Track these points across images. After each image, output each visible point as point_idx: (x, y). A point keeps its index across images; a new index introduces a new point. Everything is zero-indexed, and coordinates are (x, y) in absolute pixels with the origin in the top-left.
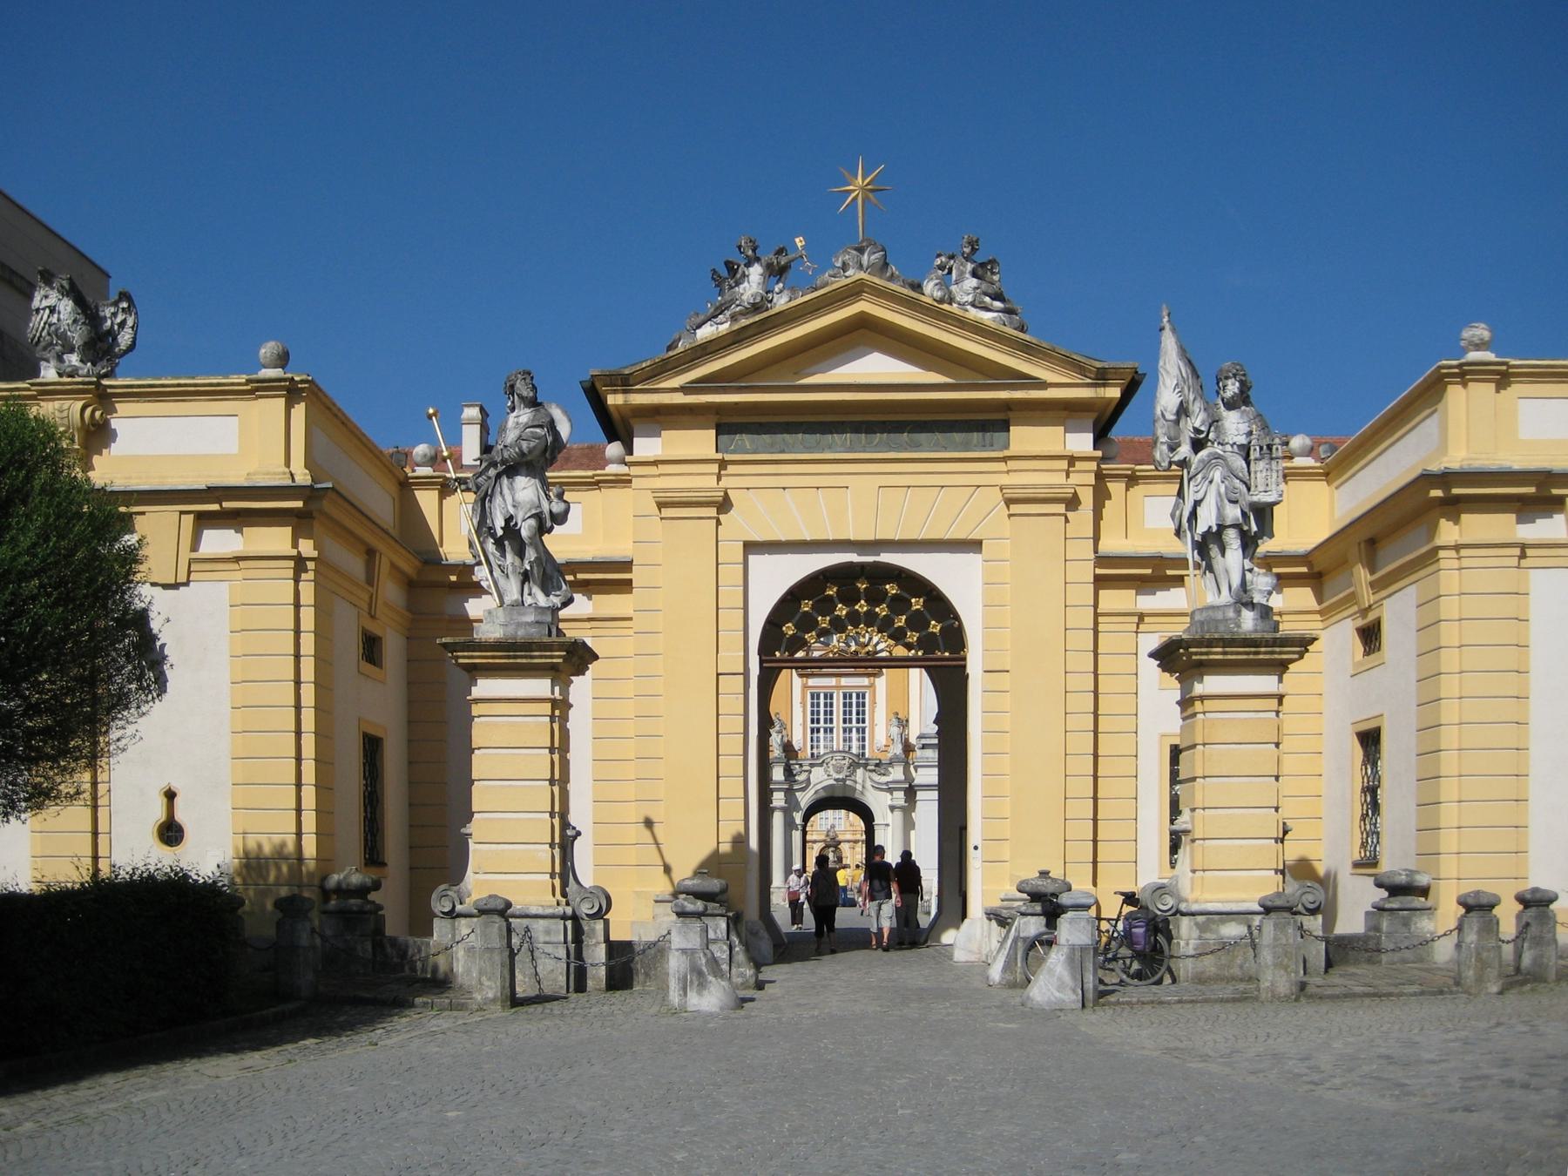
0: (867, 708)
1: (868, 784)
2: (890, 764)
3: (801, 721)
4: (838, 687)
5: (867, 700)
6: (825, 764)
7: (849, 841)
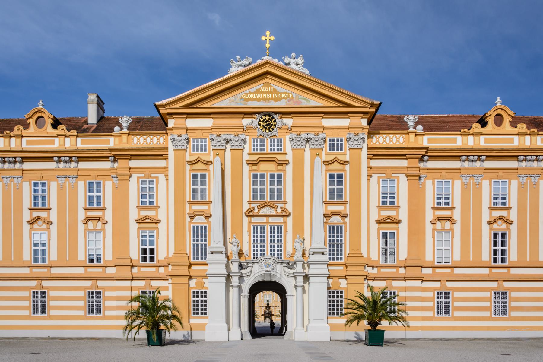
0: (283, 234)
1: (283, 274)
2: (295, 263)
3: (248, 241)
4: (267, 223)
5: (283, 230)
6: (260, 262)
7: (274, 306)
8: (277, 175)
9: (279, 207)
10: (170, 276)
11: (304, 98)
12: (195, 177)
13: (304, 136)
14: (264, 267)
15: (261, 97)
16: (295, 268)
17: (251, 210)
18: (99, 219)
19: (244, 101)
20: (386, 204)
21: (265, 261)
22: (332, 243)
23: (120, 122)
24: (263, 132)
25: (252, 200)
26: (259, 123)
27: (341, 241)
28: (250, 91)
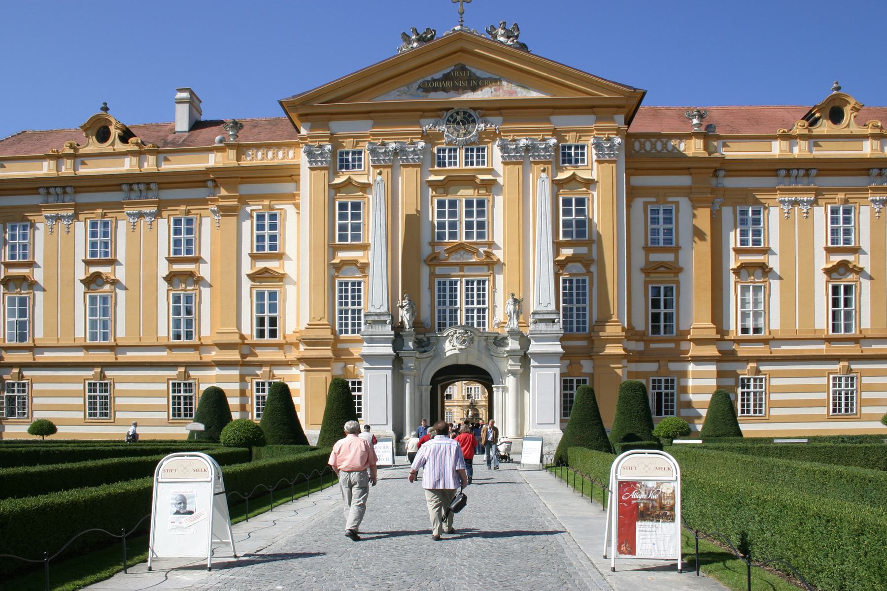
8: (477, 201)
10: (302, 360)
14: (455, 344)
19: (424, 91)
20: (659, 244)
27: (584, 301)
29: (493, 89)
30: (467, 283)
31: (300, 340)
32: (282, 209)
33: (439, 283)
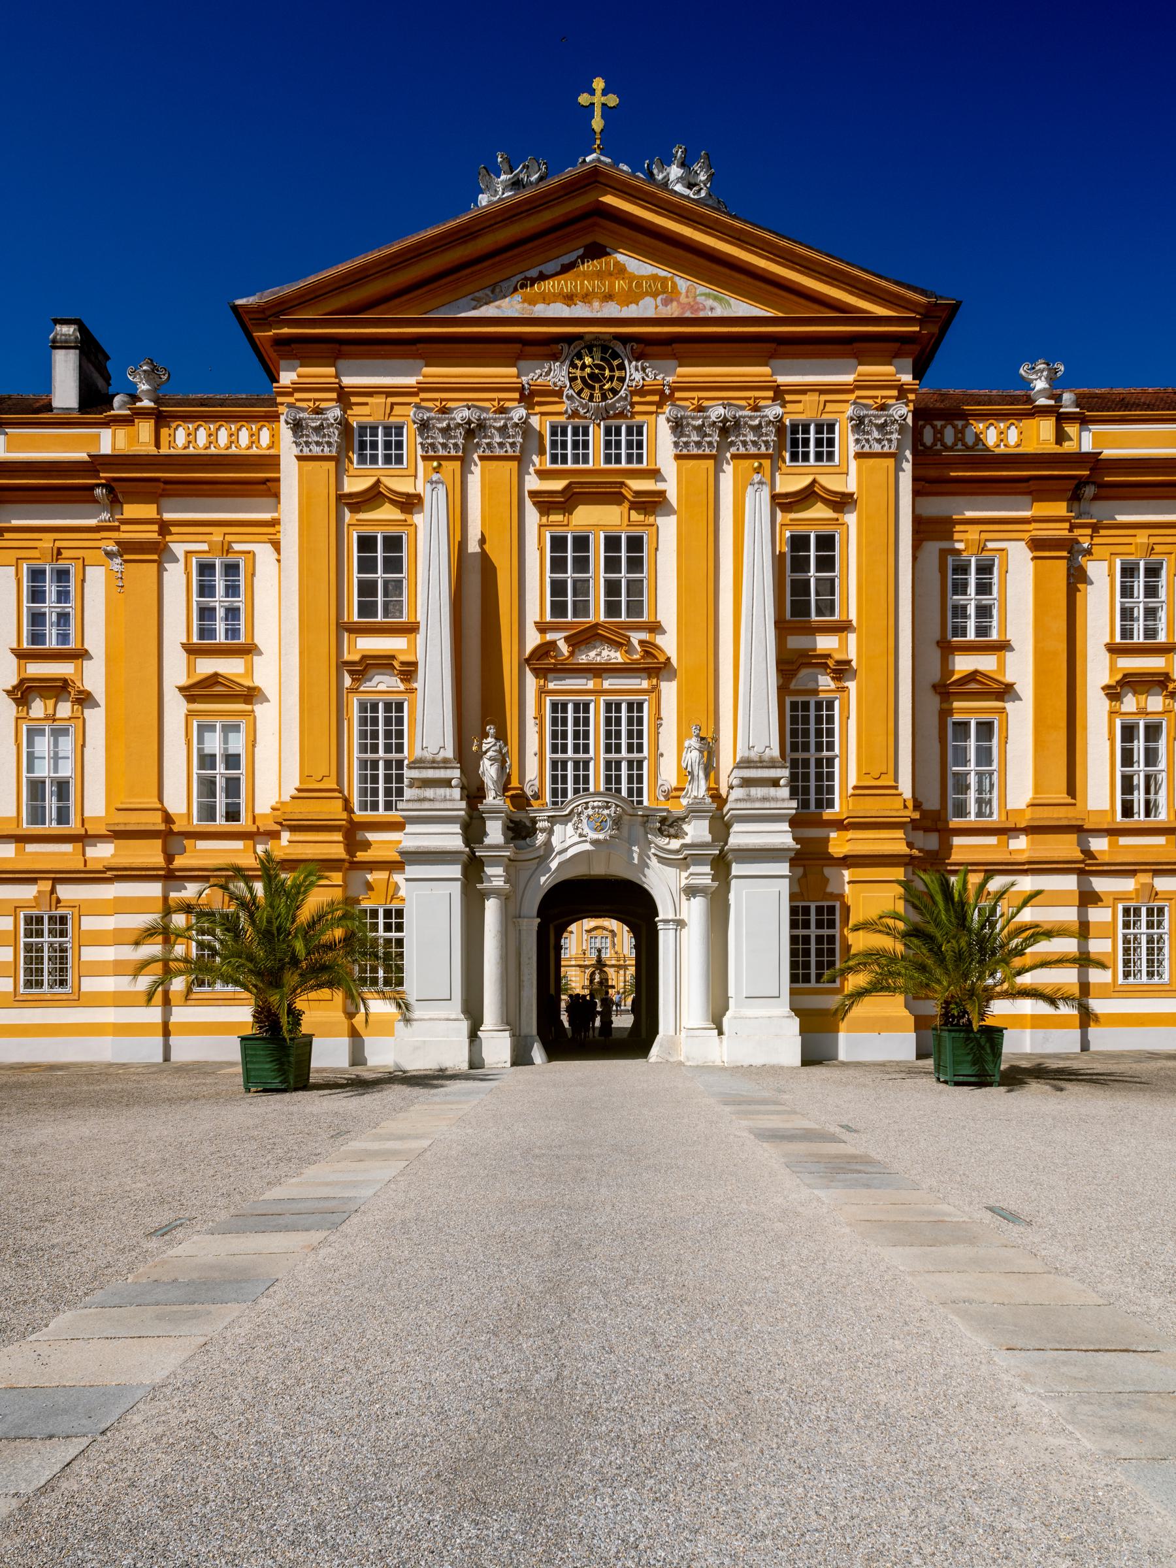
0: (645, 728)
3: (536, 748)
8: (629, 539)
9: (635, 642)
11: (714, 295)
12: (366, 543)
13: (717, 412)
14: (587, 830)
15: (576, 289)
16: (687, 834)
17: (546, 649)
18: (59, 689)
21: (590, 811)
22: (800, 755)
23: (131, 378)
24: (584, 401)
25: (548, 618)
26: (569, 373)
28: (541, 272)
29: (659, 299)
30: (608, 706)
31: (280, 824)
32: (249, 552)
33: (554, 706)
